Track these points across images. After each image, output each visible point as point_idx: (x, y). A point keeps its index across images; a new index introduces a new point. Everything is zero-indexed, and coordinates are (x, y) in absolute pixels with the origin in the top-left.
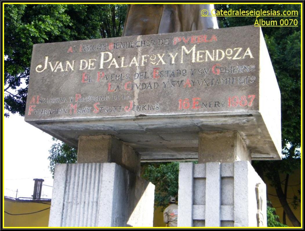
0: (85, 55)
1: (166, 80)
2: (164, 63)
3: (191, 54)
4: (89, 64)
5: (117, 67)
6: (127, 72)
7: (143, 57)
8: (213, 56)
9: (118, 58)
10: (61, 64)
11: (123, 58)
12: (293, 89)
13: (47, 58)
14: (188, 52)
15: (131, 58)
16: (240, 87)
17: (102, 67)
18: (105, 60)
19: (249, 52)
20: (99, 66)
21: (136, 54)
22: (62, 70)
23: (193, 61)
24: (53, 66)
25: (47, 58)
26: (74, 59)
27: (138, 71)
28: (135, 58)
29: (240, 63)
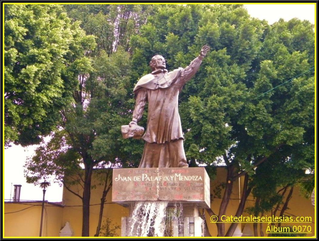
0: (136, 175)
1: (169, 187)
2: (168, 180)
3: (179, 177)
4: (137, 179)
5: (149, 180)
6: (154, 183)
7: (160, 177)
8: (187, 179)
9: (150, 177)
10: (125, 178)
11: (152, 177)
12: (212, 132)
13: (119, 175)
14: (178, 176)
15: (155, 177)
16: (197, 191)
17: (143, 180)
18: (144, 177)
19: (200, 178)
20: (142, 180)
21: (157, 175)
22: (126, 181)
23: (180, 180)
24: (122, 178)
25: (119, 175)
26: (131, 176)
27: (158, 183)
28: (156, 177)
29: (198, 182)
